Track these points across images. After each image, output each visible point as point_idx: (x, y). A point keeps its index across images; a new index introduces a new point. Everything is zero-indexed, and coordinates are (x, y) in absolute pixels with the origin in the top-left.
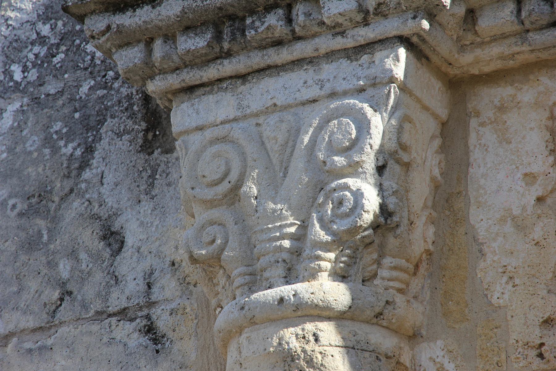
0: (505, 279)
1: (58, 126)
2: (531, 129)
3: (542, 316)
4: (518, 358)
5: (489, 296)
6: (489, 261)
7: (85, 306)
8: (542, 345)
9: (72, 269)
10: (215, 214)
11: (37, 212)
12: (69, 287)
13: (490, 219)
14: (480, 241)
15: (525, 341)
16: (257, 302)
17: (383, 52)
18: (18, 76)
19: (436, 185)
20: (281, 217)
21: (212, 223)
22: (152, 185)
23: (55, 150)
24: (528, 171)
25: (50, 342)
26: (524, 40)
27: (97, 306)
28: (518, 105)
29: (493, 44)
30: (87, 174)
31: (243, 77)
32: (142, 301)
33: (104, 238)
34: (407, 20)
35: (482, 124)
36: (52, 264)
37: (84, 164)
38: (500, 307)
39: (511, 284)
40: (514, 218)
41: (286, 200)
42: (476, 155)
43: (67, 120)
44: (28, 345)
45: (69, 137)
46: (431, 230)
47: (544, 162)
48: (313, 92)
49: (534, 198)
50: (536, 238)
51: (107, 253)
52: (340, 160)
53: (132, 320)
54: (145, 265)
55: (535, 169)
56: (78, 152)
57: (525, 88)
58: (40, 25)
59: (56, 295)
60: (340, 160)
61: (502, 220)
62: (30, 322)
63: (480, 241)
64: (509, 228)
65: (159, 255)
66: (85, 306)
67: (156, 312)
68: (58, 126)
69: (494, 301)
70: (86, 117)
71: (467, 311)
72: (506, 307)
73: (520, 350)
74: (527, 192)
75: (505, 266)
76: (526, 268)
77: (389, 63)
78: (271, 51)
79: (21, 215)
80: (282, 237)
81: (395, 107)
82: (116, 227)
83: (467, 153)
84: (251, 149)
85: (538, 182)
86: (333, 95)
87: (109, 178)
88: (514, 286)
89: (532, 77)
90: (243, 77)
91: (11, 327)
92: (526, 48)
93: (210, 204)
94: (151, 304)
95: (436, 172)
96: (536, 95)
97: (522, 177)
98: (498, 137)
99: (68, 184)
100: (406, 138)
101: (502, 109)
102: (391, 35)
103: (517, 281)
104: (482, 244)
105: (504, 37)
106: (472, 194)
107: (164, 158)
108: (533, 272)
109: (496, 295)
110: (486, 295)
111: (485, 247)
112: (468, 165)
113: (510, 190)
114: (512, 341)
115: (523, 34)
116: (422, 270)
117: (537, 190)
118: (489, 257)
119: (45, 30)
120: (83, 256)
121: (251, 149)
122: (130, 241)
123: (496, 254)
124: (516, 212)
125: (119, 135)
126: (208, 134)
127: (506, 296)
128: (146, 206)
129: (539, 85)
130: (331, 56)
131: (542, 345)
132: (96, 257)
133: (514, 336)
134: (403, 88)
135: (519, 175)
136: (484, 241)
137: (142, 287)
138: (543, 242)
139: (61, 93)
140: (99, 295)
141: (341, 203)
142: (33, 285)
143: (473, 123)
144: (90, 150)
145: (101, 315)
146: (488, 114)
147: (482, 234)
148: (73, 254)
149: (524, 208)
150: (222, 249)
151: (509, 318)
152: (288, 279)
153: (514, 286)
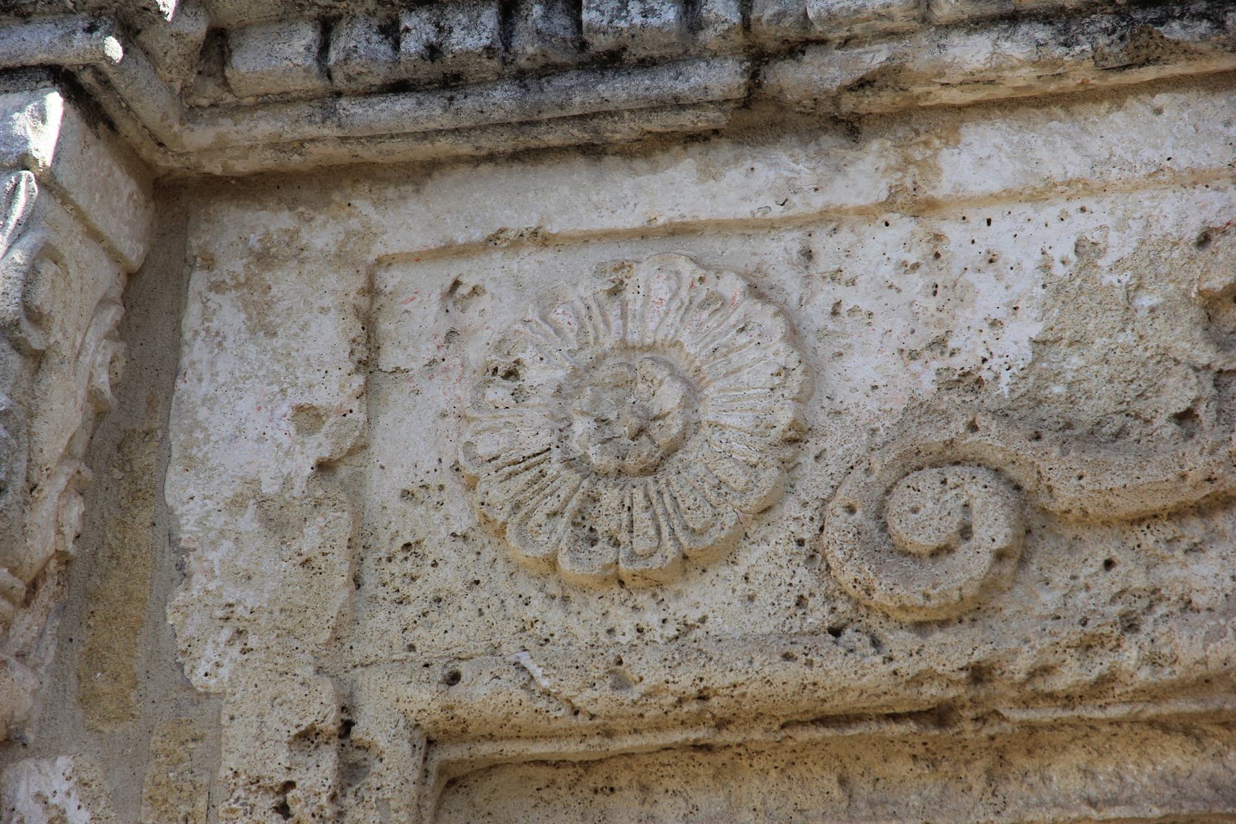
0: (226, 633)
2: (324, 310)
3: (296, 721)
4: (233, 811)
5: (187, 668)
6: (196, 590)
8: (290, 785)
13: (210, 498)
14: (182, 544)
15: (254, 774)
17: (11, 96)
19: (99, 413)
24: (305, 400)
26: (328, 114)
28: (300, 255)
29: (260, 113)
34: (74, 32)
35: (218, 287)
38: (207, 694)
39: (238, 646)
40: (262, 502)
42: (196, 353)
46: (75, 510)
47: (342, 386)
49: (312, 462)
50: (305, 550)
55: (320, 398)
57: (320, 218)
61: (237, 504)
63: (182, 544)
64: (248, 522)
69: (197, 680)
71: (133, 696)
72: (220, 695)
73: (240, 792)
74: (298, 448)
75: (231, 605)
76: (277, 614)
77: (22, 123)
81: (25, 225)
83: (176, 344)
85: (325, 429)
88: (244, 652)
89: (336, 196)
92: (329, 131)
95: (103, 380)
96: (342, 236)
97: (290, 412)
98: (250, 318)
100: (42, 296)
101: (264, 258)
102: (33, 62)
103: (253, 641)
104: (186, 551)
105: (285, 99)
106: (177, 438)
108: (289, 624)
109: (204, 667)
110: (181, 666)
111: (191, 558)
112: (176, 372)
113: (262, 438)
114: (224, 773)
115: (329, 100)
116: (44, 596)
117: (320, 446)
118: (199, 582)
123: (215, 577)
124: (269, 487)
127: (224, 672)
129: (350, 216)
131: (290, 785)
133: (231, 761)
134: (48, 183)
135: (285, 408)
136: (192, 546)
138: (319, 562)
143: (198, 281)
146: (234, 266)
147: (188, 528)
149: (287, 483)
151: (225, 720)
153: (244, 652)
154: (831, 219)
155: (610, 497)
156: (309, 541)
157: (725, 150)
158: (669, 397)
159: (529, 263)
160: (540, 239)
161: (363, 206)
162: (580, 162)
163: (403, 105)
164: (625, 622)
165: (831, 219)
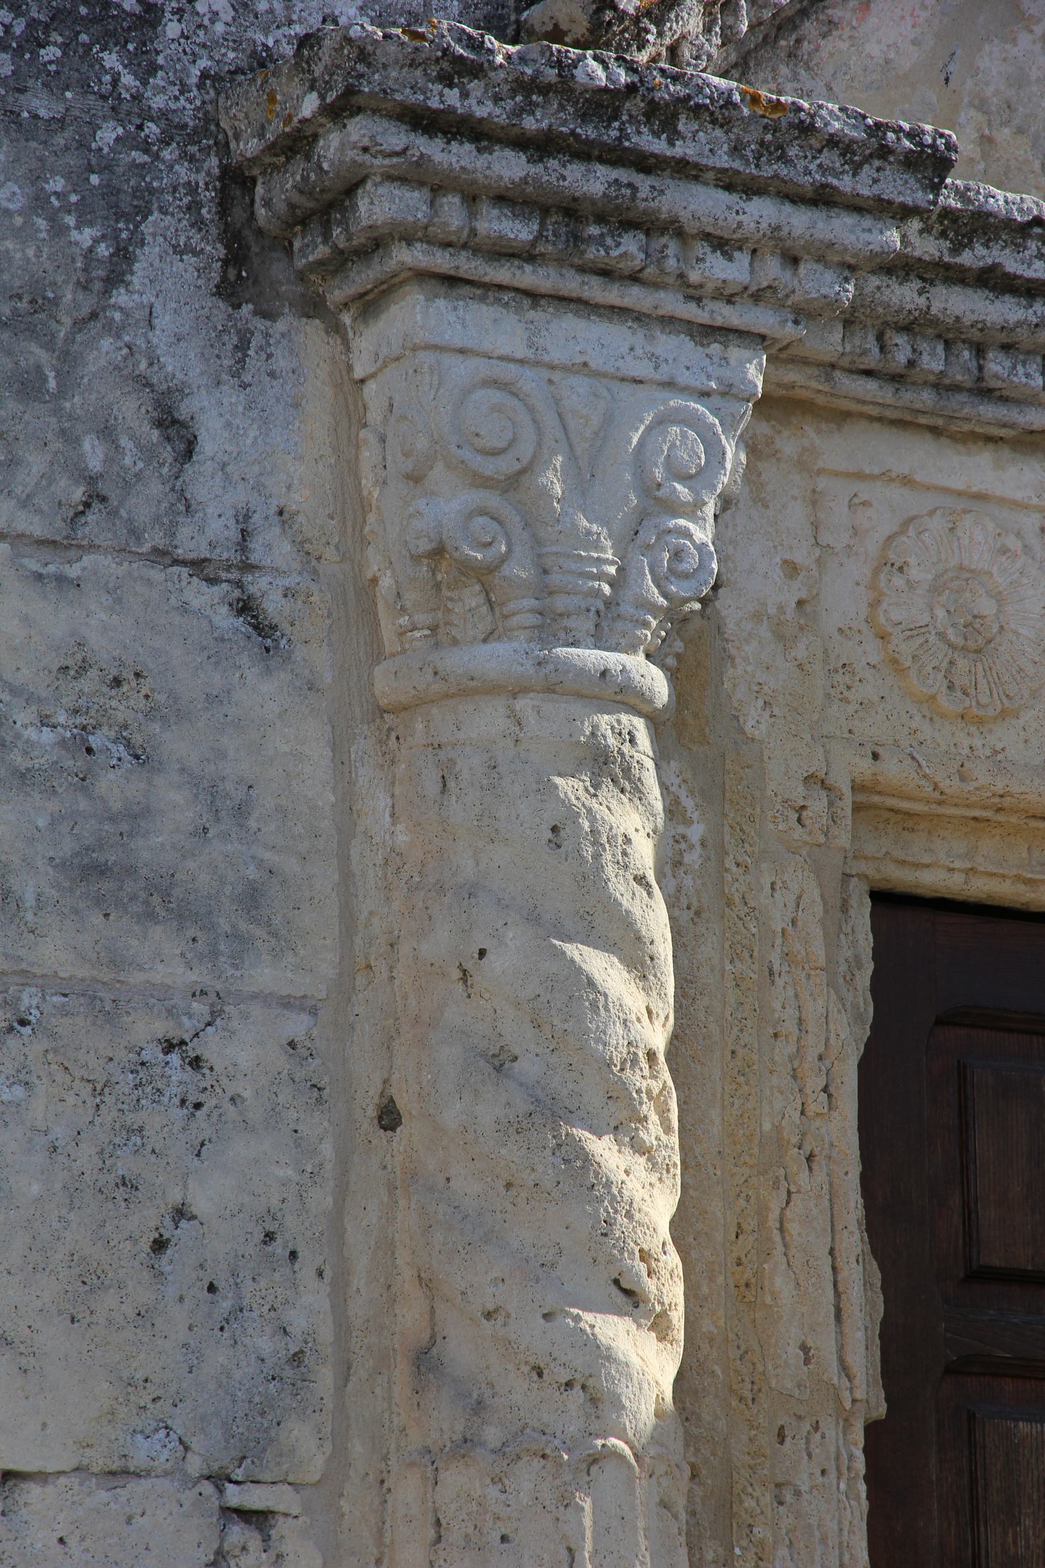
0: (760, 703)
1: (57, 184)
2: (795, 498)
3: (806, 768)
4: (776, 817)
5: (741, 720)
6: (740, 670)
7: (135, 533)
8: (803, 807)
9: (108, 460)
10: (492, 500)
11: (31, 331)
12: (103, 487)
13: (740, 609)
14: (726, 636)
15: (786, 797)
16: (567, 665)
17: (743, 351)
20: (597, 546)
21: (483, 512)
22: (242, 361)
23: (58, 230)
24: (788, 556)
25: (73, 571)
26: (829, 379)
27: (154, 538)
29: (790, 366)
30: (120, 297)
31: (534, 297)
32: (236, 558)
33: (159, 424)
34: (787, 321)
36: (73, 441)
38: (753, 740)
39: (768, 713)
41: (604, 523)
43: (77, 179)
44: (32, 565)
45: (85, 215)
47: (809, 553)
49: (796, 600)
50: (799, 657)
51: (167, 454)
53: (212, 581)
54: (240, 496)
56: (103, 250)
57: (786, 433)
59: (78, 494)
61: (757, 617)
62: (37, 528)
63: (726, 636)
64: (764, 631)
65: (258, 488)
66: (135, 533)
67: (258, 584)
68: (57, 184)
69: (748, 729)
70: (110, 191)
71: (707, 731)
72: (761, 742)
73: (778, 807)
74: (786, 587)
75: (760, 684)
76: (787, 696)
78: (595, 281)
80: (598, 577)
82: (183, 412)
84: (550, 420)
85: (800, 578)
86: (669, 385)
87: (164, 321)
88: (771, 716)
89: (794, 420)
90: (534, 297)
92: (825, 387)
93: (482, 482)
94: (248, 567)
96: (800, 450)
97: (780, 562)
98: (751, 491)
99: (87, 303)
102: (756, 331)
103: (776, 711)
104: (727, 640)
107: (260, 324)
108: (795, 704)
109: (751, 722)
110: (737, 718)
111: (730, 646)
113: (766, 576)
114: (769, 793)
115: (829, 369)
120: (124, 441)
121: (550, 420)
122: (207, 446)
123: (750, 664)
125: (179, 251)
126: (482, 368)
127: (763, 727)
128: (231, 397)
129: (803, 436)
130: (668, 322)
131: (803, 807)
132: (148, 453)
135: (778, 560)
136: (732, 638)
137: (234, 534)
138: (807, 667)
139: (61, 123)
140: (157, 519)
141: (678, 554)
142: (36, 463)
145: (164, 557)
148: (107, 433)
149: (781, 608)
150: (503, 559)
151: (766, 758)
153: (771, 716)
155: (962, 664)
156: (800, 652)
157: (1006, 453)
158: (987, 607)
159: (896, 493)
160: (907, 481)
161: (809, 430)
162: (928, 436)
163: (870, 386)
164: (966, 743)
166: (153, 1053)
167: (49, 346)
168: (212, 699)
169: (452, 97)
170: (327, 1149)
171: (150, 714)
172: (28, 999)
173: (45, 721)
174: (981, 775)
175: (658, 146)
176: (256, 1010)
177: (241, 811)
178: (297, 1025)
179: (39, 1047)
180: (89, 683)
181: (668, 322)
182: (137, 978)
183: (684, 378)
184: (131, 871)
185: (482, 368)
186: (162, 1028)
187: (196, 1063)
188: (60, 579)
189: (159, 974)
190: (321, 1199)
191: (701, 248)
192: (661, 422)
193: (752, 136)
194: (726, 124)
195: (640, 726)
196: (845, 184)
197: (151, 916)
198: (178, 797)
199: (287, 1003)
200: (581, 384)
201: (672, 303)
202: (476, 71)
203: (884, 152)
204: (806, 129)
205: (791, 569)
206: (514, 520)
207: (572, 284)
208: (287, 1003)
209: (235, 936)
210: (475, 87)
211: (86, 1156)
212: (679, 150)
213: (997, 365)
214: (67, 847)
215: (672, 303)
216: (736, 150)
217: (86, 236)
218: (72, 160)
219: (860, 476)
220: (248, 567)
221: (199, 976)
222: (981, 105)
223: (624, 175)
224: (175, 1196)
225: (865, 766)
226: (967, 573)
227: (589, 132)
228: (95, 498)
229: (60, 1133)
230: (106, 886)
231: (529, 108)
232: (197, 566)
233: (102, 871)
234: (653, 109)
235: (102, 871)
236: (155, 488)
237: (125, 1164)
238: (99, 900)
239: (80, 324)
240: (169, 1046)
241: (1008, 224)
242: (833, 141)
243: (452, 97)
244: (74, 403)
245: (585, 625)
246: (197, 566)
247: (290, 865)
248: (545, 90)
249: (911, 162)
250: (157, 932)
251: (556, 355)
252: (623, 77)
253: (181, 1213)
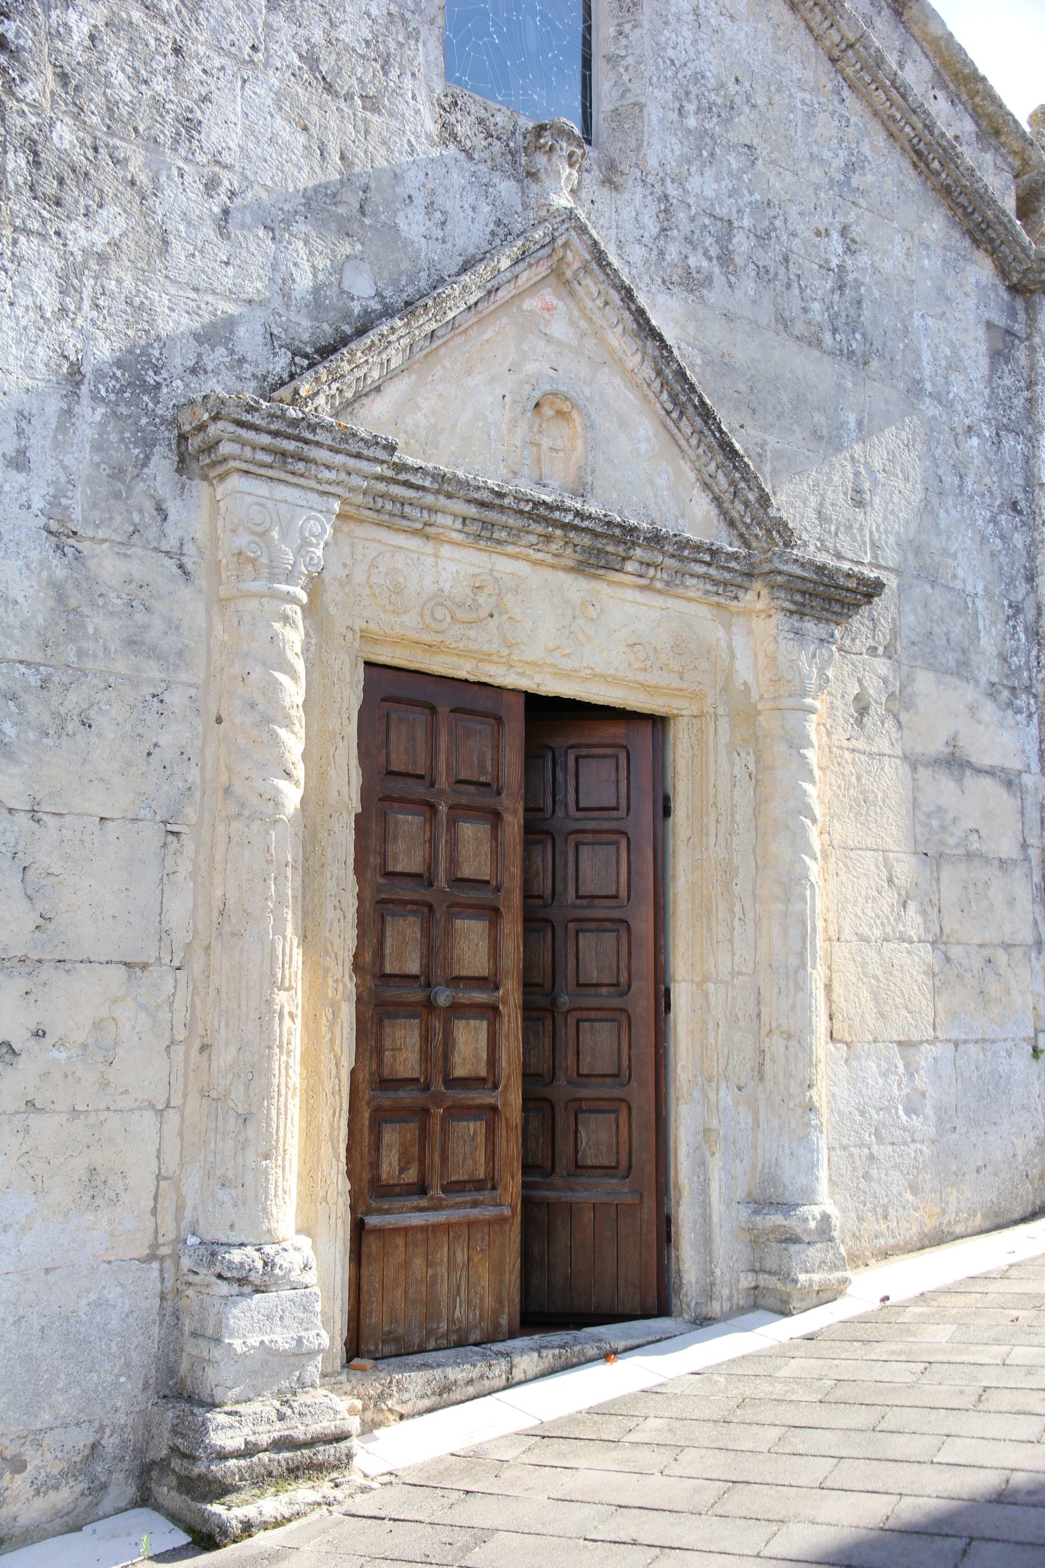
1: (128, 435)
7: (148, 542)
10: (257, 539)
11: (118, 479)
16: (278, 590)
18: (103, 393)
23: (128, 449)
25: (129, 552)
27: (154, 544)
30: (146, 470)
37: (145, 465)
43: (134, 434)
45: (136, 444)
48: (304, 503)
51: (159, 519)
52: (314, 540)
54: (181, 533)
56: (141, 456)
58: (115, 369)
59: (131, 529)
60: (314, 540)
61: (335, 579)
62: (118, 538)
66: (148, 542)
67: (185, 560)
70: (144, 438)
79: (109, 476)
82: (164, 506)
84: (275, 516)
86: (311, 508)
87: (159, 479)
90: (271, 479)
91: (106, 536)
93: (254, 533)
94: (182, 554)
99: (136, 472)
119: (119, 373)
121: (275, 516)
122: (171, 517)
126: (255, 499)
128: (179, 503)
130: (312, 489)
132: (153, 518)
141: (311, 559)
142: (119, 519)
144: (147, 458)
145: (156, 550)
148: (141, 511)
152: (287, 583)
154: (423, 553)
156: (347, 590)
158: (401, 580)
159: (376, 545)
160: (380, 542)
163: (370, 513)
165: (423, 553)
166: (149, 698)
167: (124, 483)
168: (170, 594)
169: (249, 417)
170: (200, 728)
171: (151, 597)
172: (112, 680)
173: (119, 597)
174: (397, 629)
175: (310, 436)
176: (180, 687)
177: (178, 628)
178: (193, 692)
179: (114, 694)
180: (133, 586)
181: (312, 489)
182: (145, 675)
183: (315, 506)
184: (144, 643)
185: (255, 499)
186: (152, 691)
187: (162, 701)
188: (125, 555)
189: (151, 674)
190: (198, 743)
191: (322, 468)
192: (308, 519)
193: (339, 436)
194: (331, 432)
195: (298, 609)
196: (365, 452)
197: (149, 657)
198: (159, 622)
199: (190, 685)
200: (285, 506)
201: (313, 484)
202: (257, 410)
203: (377, 443)
204: (354, 435)
205: (345, 565)
206: (263, 545)
207: (283, 476)
208: (190, 685)
209: (174, 664)
210: (256, 414)
211: (128, 727)
212: (317, 438)
213: (407, 509)
214: (125, 635)
215: (313, 484)
216: (334, 439)
217: (136, 451)
218: (133, 428)
219: (366, 539)
220: (182, 554)
221: (163, 676)
222: (406, 432)
223: (300, 444)
224: (154, 740)
225: (364, 625)
226: (396, 570)
227: (290, 431)
228: (136, 531)
229: (120, 720)
230: (136, 647)
231: (273, 422)
232: (167, 553)
233: (135, 643)
234: (309, 425)
235: (135, 643)
236: (155, 529)
237: (139, 730)
238: (134, 651)
239: (133, 478)
240: (154, 696)
241: (412, 468)
242: (362, 439)
243: (249, 417)
244: (130, 502)
245: (283, 578)
246: (167, 553)
247: (192, 644)
248: (277, 417)
249: (385, 447)
250: (151, 662)
251: (277, 497)
252: (301, 415)
253: (156, 745)
